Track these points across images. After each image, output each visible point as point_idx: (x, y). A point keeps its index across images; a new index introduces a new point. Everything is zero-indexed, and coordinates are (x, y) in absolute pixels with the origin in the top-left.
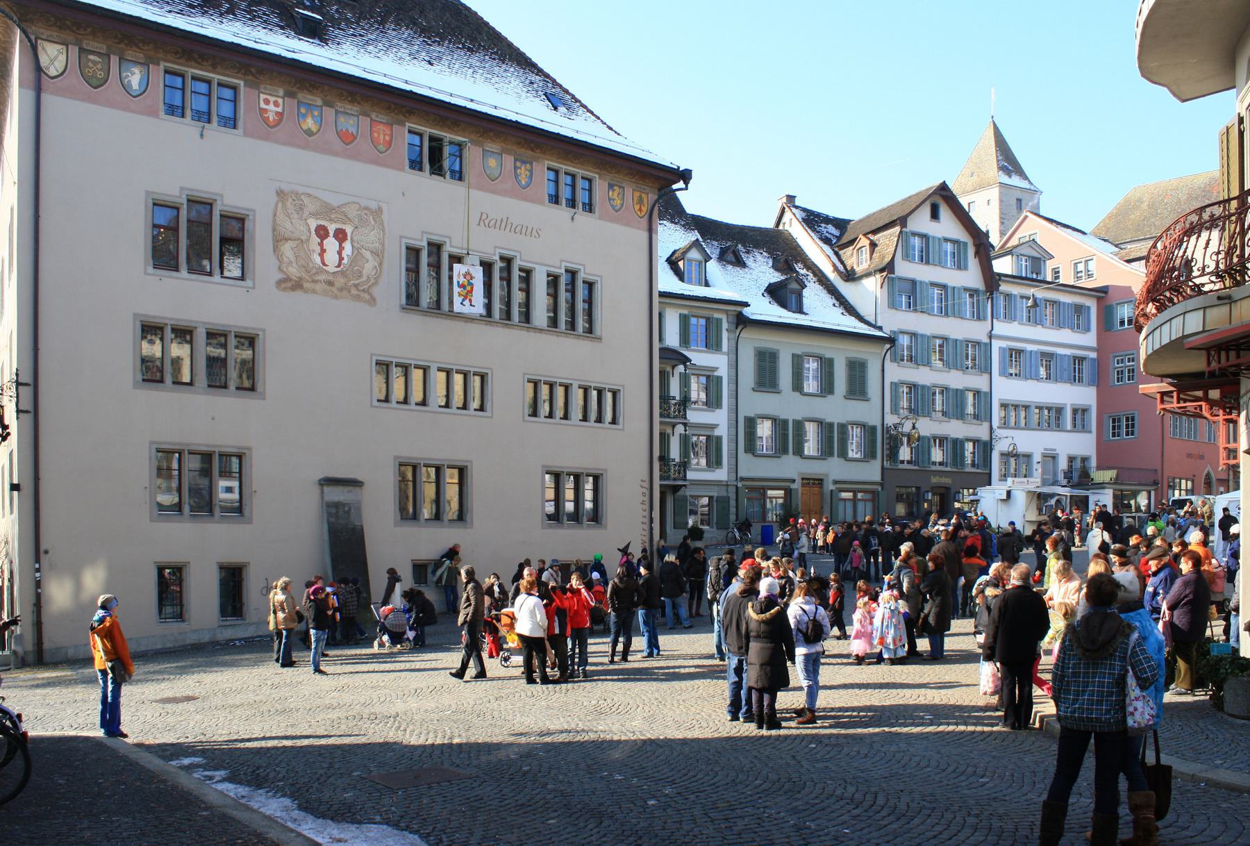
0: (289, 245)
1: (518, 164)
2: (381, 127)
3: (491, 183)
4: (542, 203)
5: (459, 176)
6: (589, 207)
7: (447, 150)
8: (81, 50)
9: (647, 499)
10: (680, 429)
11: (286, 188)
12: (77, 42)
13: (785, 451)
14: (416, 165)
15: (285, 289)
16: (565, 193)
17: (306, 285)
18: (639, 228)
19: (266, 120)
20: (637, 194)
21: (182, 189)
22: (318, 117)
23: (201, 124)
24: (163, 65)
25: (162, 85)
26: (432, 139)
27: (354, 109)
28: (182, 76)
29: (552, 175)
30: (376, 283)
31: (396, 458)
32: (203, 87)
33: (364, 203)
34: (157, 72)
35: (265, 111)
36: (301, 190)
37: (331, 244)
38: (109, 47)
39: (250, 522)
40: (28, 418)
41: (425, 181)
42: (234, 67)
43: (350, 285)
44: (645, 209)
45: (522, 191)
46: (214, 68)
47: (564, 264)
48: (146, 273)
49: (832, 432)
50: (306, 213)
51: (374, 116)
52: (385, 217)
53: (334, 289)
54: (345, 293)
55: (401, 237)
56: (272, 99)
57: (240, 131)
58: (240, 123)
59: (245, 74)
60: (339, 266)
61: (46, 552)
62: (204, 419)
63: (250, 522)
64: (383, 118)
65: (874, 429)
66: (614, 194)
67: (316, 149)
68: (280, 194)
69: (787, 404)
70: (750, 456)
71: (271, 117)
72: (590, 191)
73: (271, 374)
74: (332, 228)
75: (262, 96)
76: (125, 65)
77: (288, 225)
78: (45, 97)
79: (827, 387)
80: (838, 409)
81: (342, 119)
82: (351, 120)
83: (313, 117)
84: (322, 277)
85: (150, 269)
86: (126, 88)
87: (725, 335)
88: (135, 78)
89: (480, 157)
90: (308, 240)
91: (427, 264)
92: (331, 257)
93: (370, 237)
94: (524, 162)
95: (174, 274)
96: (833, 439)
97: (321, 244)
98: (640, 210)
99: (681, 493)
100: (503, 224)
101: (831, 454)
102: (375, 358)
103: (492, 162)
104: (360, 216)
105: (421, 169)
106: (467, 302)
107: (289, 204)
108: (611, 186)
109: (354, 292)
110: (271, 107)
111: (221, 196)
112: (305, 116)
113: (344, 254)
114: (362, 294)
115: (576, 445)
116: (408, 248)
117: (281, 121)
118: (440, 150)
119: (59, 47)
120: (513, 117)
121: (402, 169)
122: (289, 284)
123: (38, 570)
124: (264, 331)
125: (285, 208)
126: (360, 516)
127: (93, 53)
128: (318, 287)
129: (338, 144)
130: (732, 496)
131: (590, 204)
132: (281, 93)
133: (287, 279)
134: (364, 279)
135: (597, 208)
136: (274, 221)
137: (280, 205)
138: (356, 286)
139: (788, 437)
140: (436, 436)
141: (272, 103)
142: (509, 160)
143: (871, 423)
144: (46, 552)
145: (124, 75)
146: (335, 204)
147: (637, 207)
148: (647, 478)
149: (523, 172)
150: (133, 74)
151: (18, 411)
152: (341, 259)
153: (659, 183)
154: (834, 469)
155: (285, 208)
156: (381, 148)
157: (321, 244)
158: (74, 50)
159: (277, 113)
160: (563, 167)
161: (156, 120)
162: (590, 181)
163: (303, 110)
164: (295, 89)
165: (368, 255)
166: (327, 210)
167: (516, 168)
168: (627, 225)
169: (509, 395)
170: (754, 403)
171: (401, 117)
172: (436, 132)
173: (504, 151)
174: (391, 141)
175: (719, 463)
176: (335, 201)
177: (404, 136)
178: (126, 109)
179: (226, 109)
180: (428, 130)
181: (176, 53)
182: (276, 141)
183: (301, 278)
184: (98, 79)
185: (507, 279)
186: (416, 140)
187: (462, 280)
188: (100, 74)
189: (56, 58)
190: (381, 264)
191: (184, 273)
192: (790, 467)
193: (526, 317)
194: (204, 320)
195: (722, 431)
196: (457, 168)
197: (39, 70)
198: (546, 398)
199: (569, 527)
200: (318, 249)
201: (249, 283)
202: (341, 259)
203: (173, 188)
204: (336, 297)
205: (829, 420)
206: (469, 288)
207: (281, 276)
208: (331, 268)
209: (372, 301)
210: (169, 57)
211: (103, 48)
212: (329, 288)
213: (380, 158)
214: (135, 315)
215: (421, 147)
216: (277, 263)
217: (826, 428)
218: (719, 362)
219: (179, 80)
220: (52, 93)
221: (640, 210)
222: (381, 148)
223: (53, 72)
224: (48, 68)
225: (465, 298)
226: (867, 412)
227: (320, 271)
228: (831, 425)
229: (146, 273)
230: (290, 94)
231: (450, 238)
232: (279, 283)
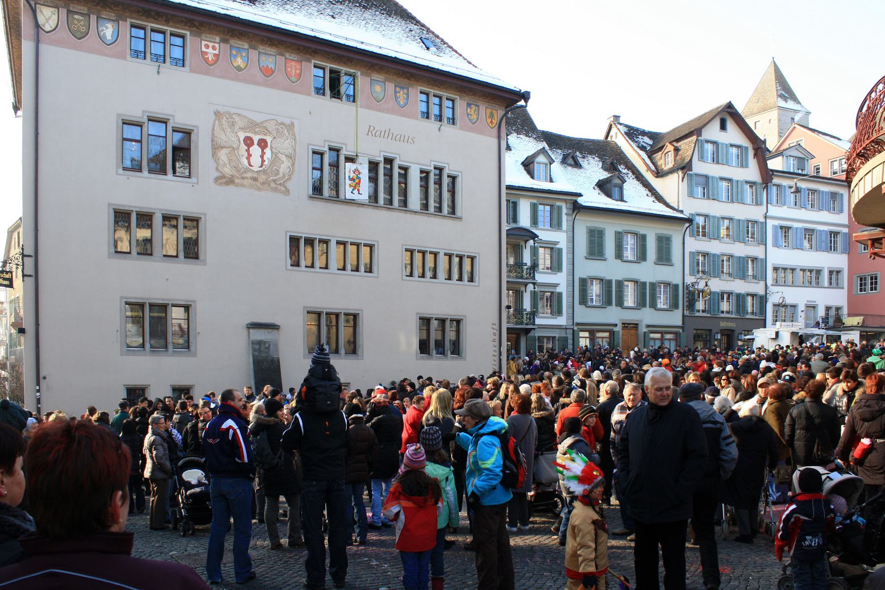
0: (224, 151)
1: (398, 89)
2: (293, 63)
3: (376, 104)
4: (417, 118)
5: (353, 99)
6: (453, 121)
7: (344, 79)
8: (69, 12)
9: (497, 338)
10: (530, 287)
11: (221, 109)
12: (66, 6)
13: (609, 302)
14: (320, 91)
15: (221, 184)
16: (435, 110)
17: (237, 181)
18: (490, 136)
19: (206, 60)
20: (489, 111)
21: (144, 112)
22: (244, 56)
23: (158, 64)
24: (129, 21)
25: (128, 36)
26: (332, 71)
27: (272, 51)
28: (144, 29)
29: (424, 97)
30: (289, 179)
31: (305, 307)
32: (160, 37)
33: (280, 120)
34: (125, 26)
35: (206, 53)
36: (233, 111)
37: (256, 150)
38: (89, 9)
39: (195, 355)
40: (31, 281)
41: (327, 103)
42: (182, 21)
43: (271, 181)
44: (495, 122)
45: (401, 110)
46: (167, 22)
47: (433, 163)
48: (117, 174)
49: (645, 289)
50: (237, 128)
51: (287, 55)
52: (296, 130)
53: (258, 184)
54: (266, 186)
55: (309, 144)
56: (211, 45)
57: (187, 68)
58: (187, 63)
59: (190, 27)
60: (261, 166)
61: (45, 378)
62: (160, 279)
63: (195, 355)
64: (294, 57)
65: (677, 286)
66: (472, 111)
67: (245, 81)
68: (217, 114)
69: (610, 268)
70: (583, 307)
71: (210, 57)
72: (453, 109)
73: (209, 247)
74: (256, 139)
75: (204, 43)
76: (101, 22)
77: (223, 137)
78: (42, 47)
79: (642, 256)
80: (649, 272)
81: (263, 58)
82: (270, 58)
83: (242, 57)
84: (249, 175)
85: (121, 171)
86: (102, 38)
87: (564, 218)
88: (108, 30)
89: (366, 84)
90: (238, 148)
91: (329, 163)
92: (256, 160)
93: (284, 145)
94: (402, 88)
95: (139, 174)
96: (646, 294)
97: (248, 151)
98: (491, 122)
99: (531, 334)
100: (387, 134)
101: (644, 306)
102: (288, 234)
103: (378, 88)
104: (277, 129)
105: (324, 94)
106: (356, 191)
107: (224, 121)
108: (469, 105)
109: (273, 185)
110: (210, 50)
111: (173, 116)
112: (235, 56)
113: (265, 158)
114: (279, 187)
115: (441, 298)
116: (314, 152)
117: (218, 60)
118: (339, 80)
119: (52, 9)
120: (393, 54)
121: (309, 95)
122: (224, 180)
123: (38, 391)
124: (205, 214)
125: (221, 124)
126: (277, 350)
127: (77, 13)
128: (246, 182)
129: (260, 76)
130: (570, 337)
131: (453, 119)
132: (218, 39)
133: (223, 177)
134: (281, 175)
135: (458, 121)
136: (213, 134)
137: (217, 122)
138: (275, 181)
139: (612, 293)
140: (335, 291)
141: (211, 46)
142: (390, 87)
143: (675, 282)
144: (45, 378)
145: (100, 29)
146: (259, 121)
148: (497, 322)
149: (401, 95)
150: (107, 28)
151: (24, 276)
152: (263, 161)
153: (507, 105)
154: (647, 317)
155: (221, 124)
156: (293, 79)
157: (248, 151)
158: (63, 12)
159: (215, 55)
160: (432, 91)
161: (124, 62)
162: (453, 101)
163: (234, 52)
164: (227, 37)
165: (283, 158)
166: (252, 125)
167: (396, 92)
168: (481, 133)
169: (391, 260)
170: (587, 268)
171: (308, 56)
172: (335, 66)
173: (386, 80)
174: (300, 75)
175: (560, 313)
176: (258, 118)
178: (102, 53)
179: (177, 53)
180: (329, 65)
181: (139, 12)
182: (214, 76)
183: (232, 176)
184: (81, 33)
185: (389, 175)
186: (320, 73)
187: (352, 175)
188: (83, 29)
189: (49, 18)
190: (293, 165)
191: (145, 173)
192: (613, 316)
193: (404, 203)
194: (160, 207)
195: (563, 289)
196: (352, 93)
197: (37, 26)
198: (421, 263)
199: (437, 358)
200: (246, 154)
201: (194, 180)
202: (263, 161)
203: (136, 113)
204: (259, 189)
205: (642, 280)
206: (357, 181)
207: (218, 174)
208: (256, 168)
209: (287, 192)
210: (134, 15)
211: (85, 10)
212: (254, 183)
213: (293, 85)
214: (109, 204)
215: (324, 78)
216: (215, 165)
217: (641, 286)
218: (560, 238)
219: (142, 32)
220: (47, 44)
221: (491, 122)
222: (293, 79)
223: (48, 28)
224: (44, 25)
225: (355, 188)
226: (672, 274)
227: (247, 170)
228: (644, 284)
229: (117, 174)
230: (224, 41)
231: (345, 144)
232: (217, 180)
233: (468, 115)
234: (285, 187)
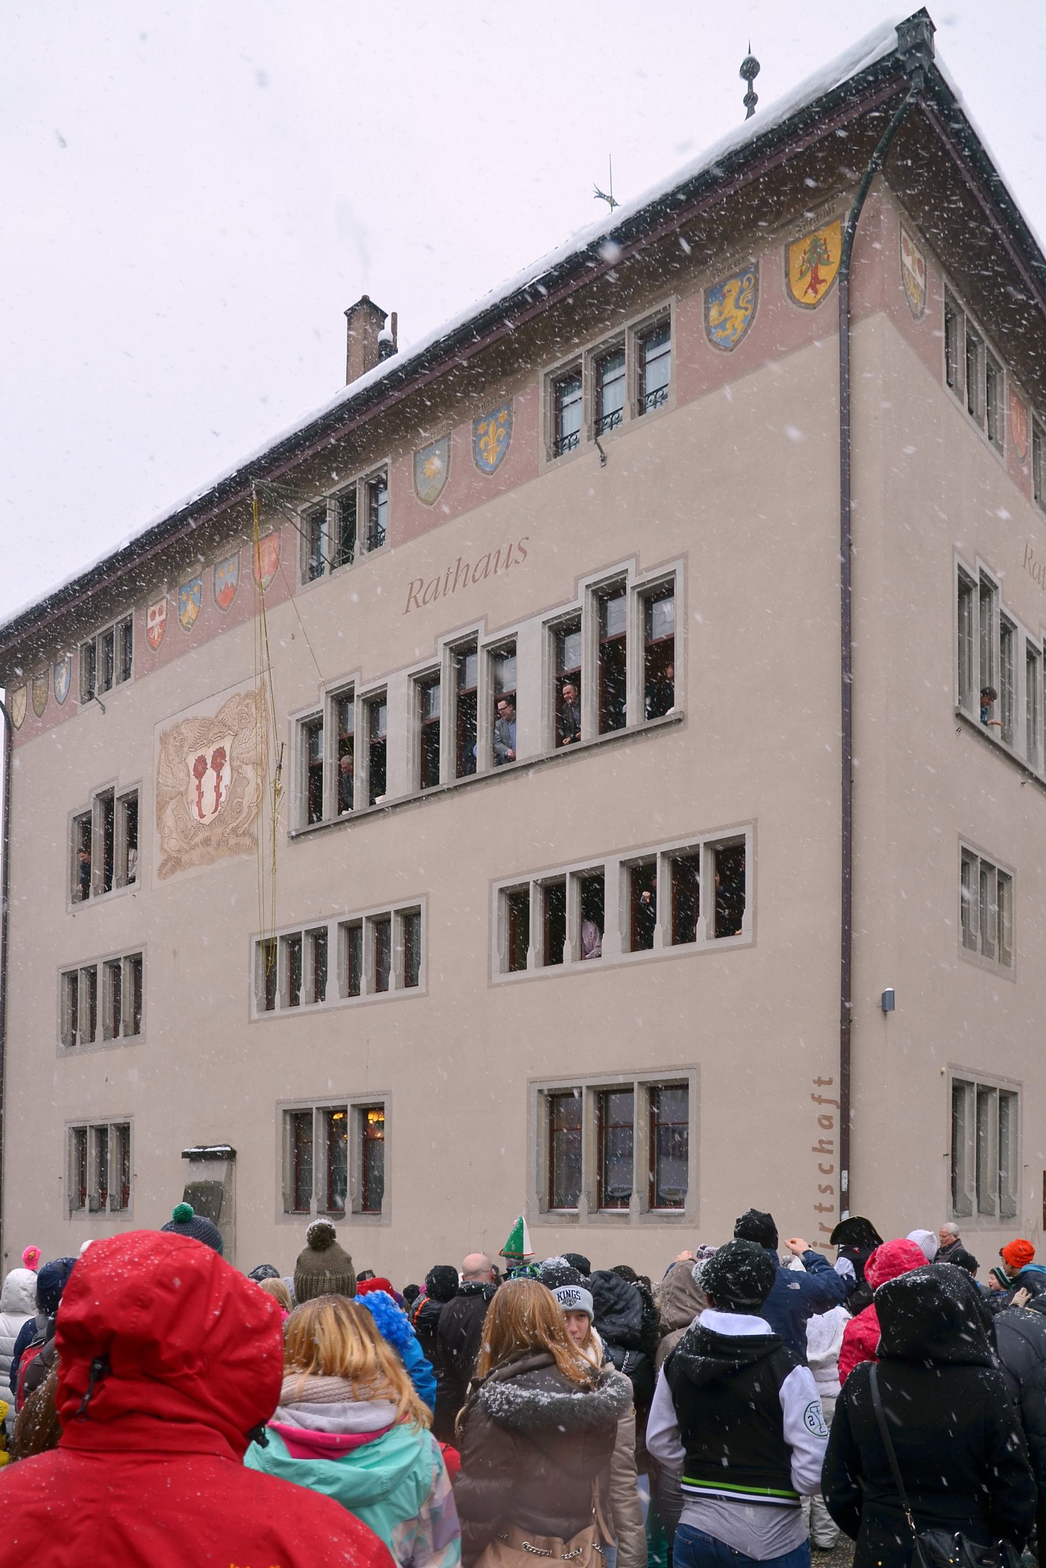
74: (209, 753)
134: (246, 810)
138: (234, 830)
157: (199, 787)
165: (249, 771)
177: (277, 546)
200: (194, 795)
202: (219, 795)
234: (251, 836)
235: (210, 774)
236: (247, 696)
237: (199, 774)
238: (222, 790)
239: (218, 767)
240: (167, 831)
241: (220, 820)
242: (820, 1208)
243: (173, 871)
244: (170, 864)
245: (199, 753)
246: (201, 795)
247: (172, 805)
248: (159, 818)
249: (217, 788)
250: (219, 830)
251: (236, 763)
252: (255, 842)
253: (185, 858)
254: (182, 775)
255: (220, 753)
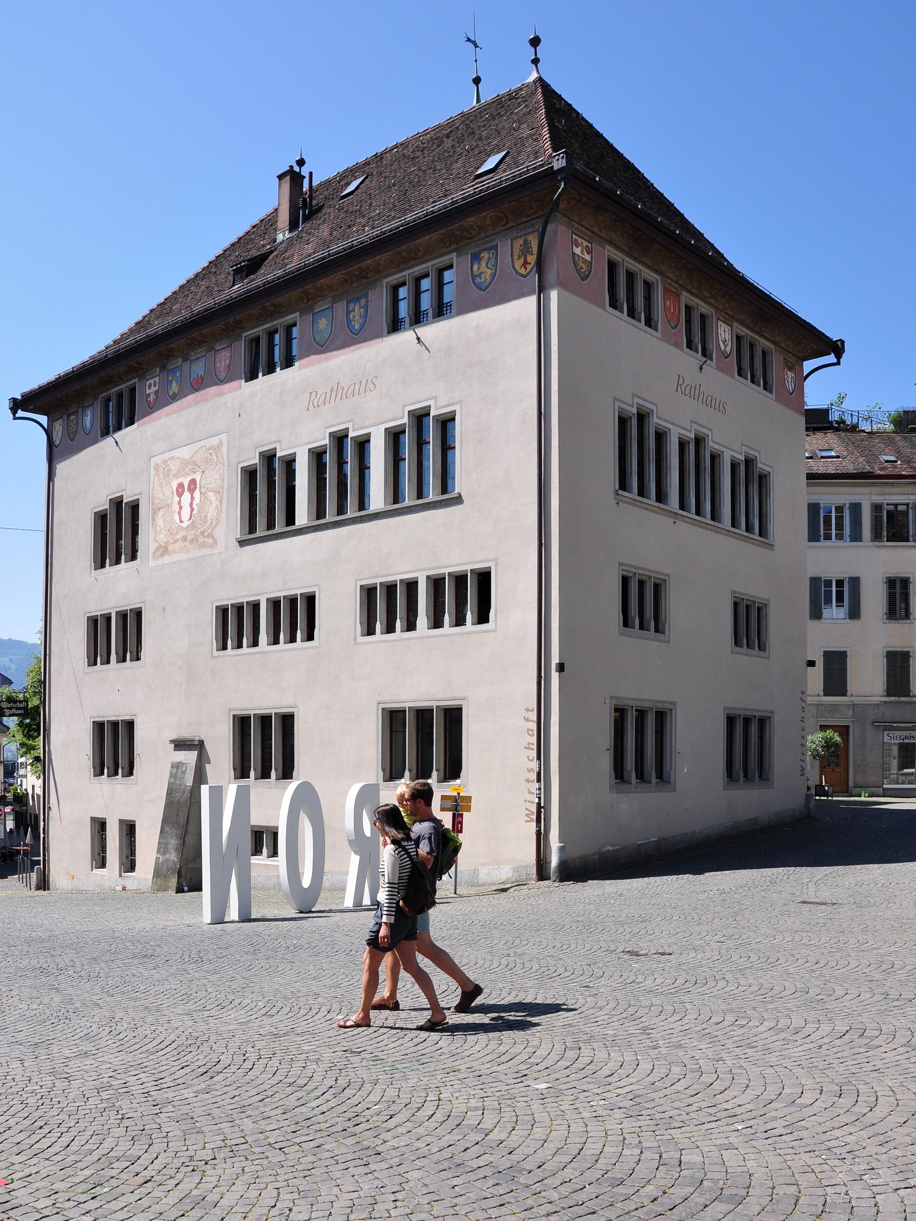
74: (186, 482)
109: (201, 540)
138: (202, 533)
147: (518, 264)
157: (179, 503)
165: (211, 495)
200: (177, 508)
202: (192, 510)
221: (525, 263)
233: (473, 277)
234: (213, 537)
235: (187, 496)
236: (211, 448)
237: (180, 495)
238: (194, 506)
239: (192, 490)
240: (158, 528)
241: (193, 526)
242: (528, 781)
243: (162, 555)
244: (160, 552)
245: (180, 480)
246: (181, 508)
247: (162, 512)
248: (154, 519)
249: (191, 505)
250: (193, 532)
251: (203, 490)
252: (215, 541)
253: (170, 548)
254: (168, 493)
255: (193, 482)
